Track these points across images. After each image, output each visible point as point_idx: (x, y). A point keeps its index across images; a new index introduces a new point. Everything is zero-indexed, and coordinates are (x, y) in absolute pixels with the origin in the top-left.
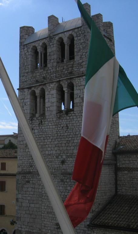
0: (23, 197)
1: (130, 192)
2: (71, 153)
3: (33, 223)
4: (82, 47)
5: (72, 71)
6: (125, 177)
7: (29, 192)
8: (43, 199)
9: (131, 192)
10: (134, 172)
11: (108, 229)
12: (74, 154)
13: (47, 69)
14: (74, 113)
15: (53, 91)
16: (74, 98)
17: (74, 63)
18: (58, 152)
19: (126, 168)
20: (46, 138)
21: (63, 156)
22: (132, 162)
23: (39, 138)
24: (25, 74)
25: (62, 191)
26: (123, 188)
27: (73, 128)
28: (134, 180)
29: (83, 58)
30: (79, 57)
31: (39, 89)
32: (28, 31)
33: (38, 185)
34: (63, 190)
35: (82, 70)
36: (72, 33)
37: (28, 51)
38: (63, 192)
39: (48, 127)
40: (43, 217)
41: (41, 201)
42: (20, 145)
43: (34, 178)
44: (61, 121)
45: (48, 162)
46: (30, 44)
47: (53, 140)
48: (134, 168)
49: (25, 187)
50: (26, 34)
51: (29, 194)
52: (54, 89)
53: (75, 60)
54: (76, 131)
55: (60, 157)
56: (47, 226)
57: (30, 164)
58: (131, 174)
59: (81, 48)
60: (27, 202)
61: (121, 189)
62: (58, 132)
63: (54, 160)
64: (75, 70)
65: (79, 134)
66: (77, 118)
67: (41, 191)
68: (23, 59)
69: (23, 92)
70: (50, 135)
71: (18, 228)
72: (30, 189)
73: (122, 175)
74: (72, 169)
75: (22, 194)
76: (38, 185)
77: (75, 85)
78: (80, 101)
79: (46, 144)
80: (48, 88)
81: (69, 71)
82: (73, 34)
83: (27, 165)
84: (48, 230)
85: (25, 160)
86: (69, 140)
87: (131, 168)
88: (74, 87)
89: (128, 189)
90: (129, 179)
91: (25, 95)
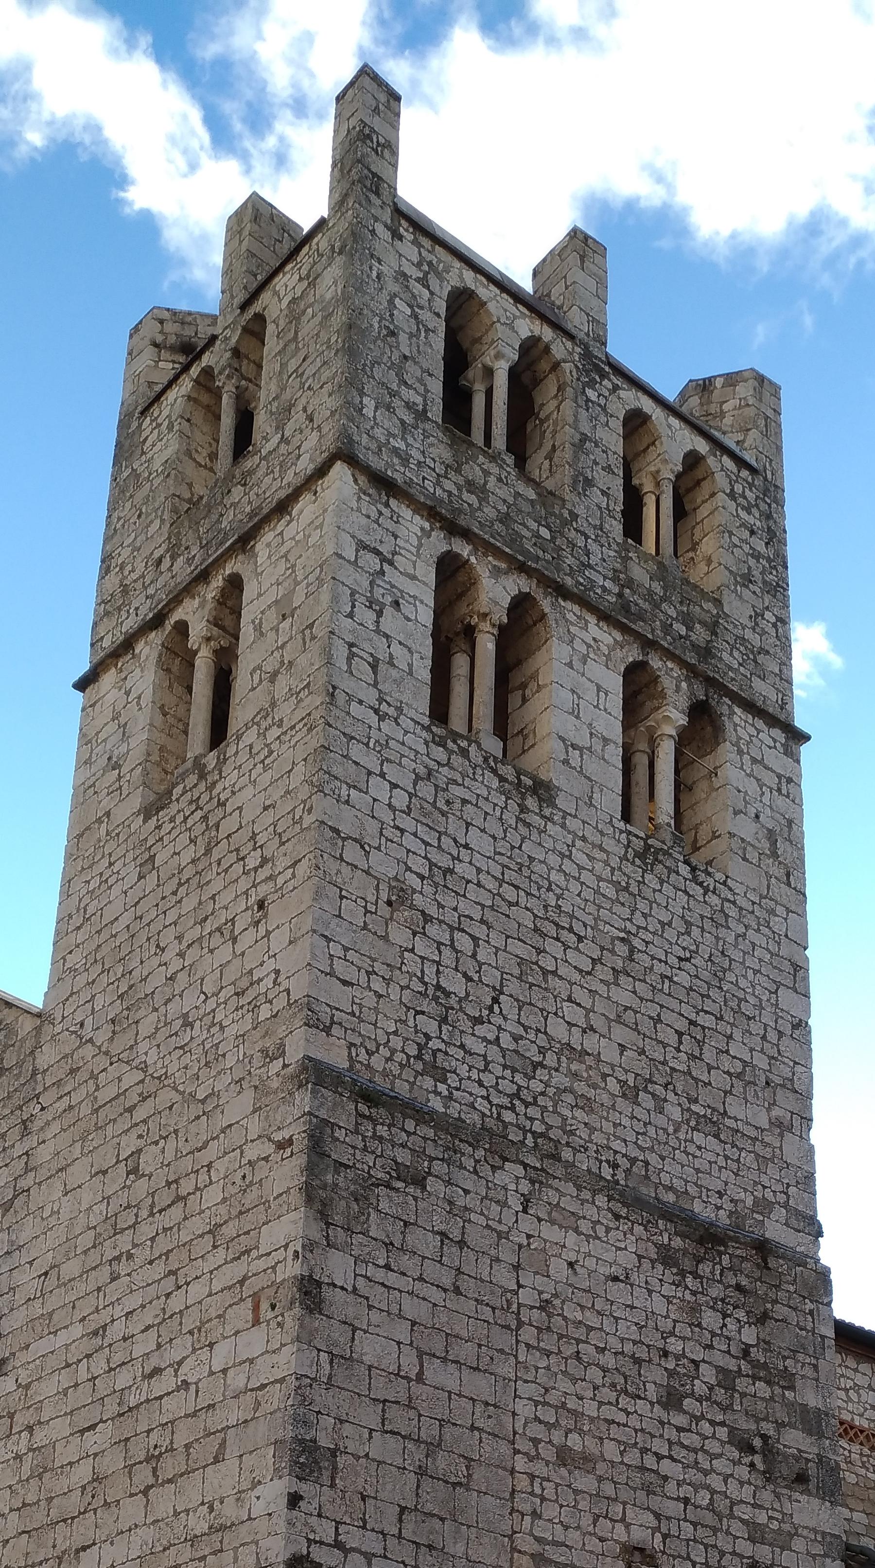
0: (361, 1282)
3: (442, 1520)
7: (417, 1260)
25: (670, 1324)
39: (568, 866)
43: (462, 1167)
45: (569, 1099)
57: (420, 1047)
63: (605, 1098)
76: (488, 1226)
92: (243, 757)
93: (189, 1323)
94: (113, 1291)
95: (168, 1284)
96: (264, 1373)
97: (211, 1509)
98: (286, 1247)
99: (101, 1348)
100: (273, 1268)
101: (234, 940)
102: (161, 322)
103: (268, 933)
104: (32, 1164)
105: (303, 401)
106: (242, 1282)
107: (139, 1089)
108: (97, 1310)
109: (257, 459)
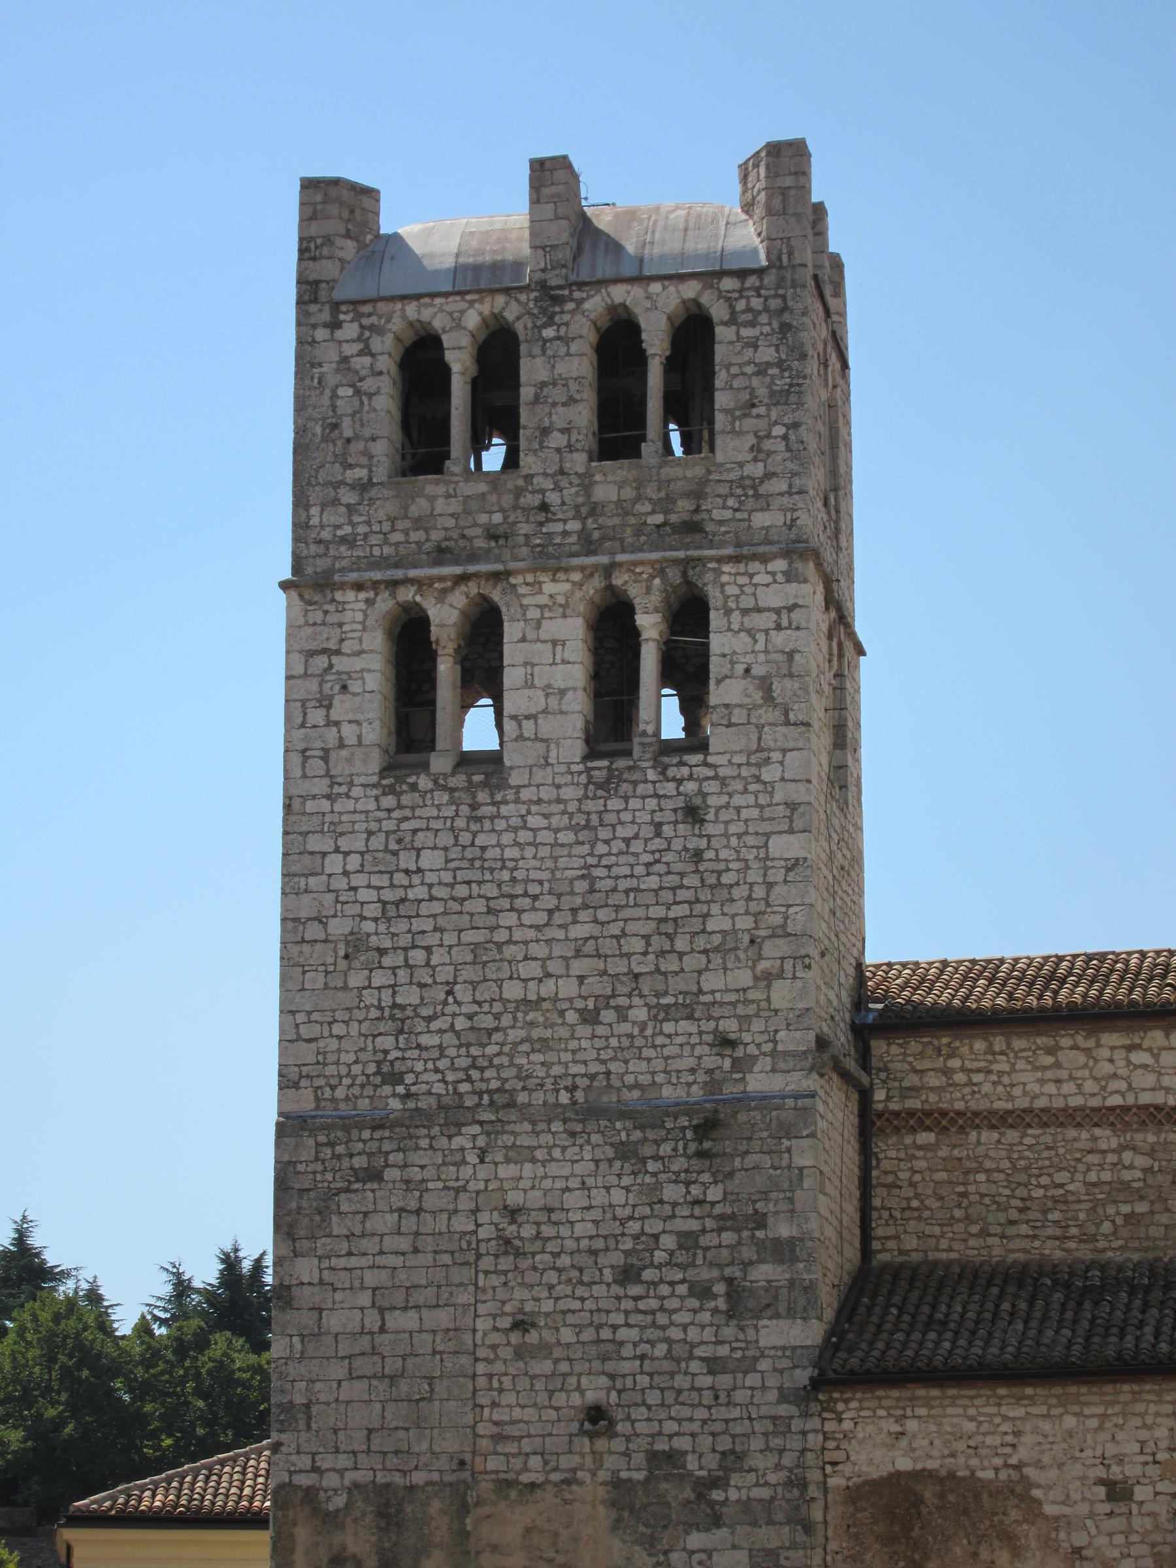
0: (326, 1273)
1: (950, 1250)
2: (686, 993)
3: (407, 1429)
4: (769, 387)
5: (696, 518)
6: (921, 1164)
7: (377, 1239)
8: (486, 1273)
9: (956, 1246)
10: (973, 1135)
11: (921, 1392)
12: (703, 999)
13: (521, 482)
14: (705, 764)
15: (560, 620)
16: (708, 678)
17: (709, 472)
18: (596, 985)
19: (928, 1114)
20: (505, 903)
21: (630, 1007)
22: (960, 1077)
23: (456, 907)
24: (343, 490)
26: (905, 1232)
27: (703, 851)
28: (971, 1178)
29: (769, 453)
30: (748, 445)
31: (459, 599)
32: (358, 215)
33: (446, 1188)
34: (634, 1206)
35: (761, 519)
36: (700, 293)
37: (367, 346)
38: (631, 1218)
39: (524, 836)
40: (482, 1382)
41: (471, 1288)
42: (306, 948)
43: (417, 1148)
44: (615, 804)
45: (525, 1047)
46: (382, 307)
47: (558, 918)
48: (976, 1114)
49: (344, 1207)
50: (348, 235)
51: (377, 1249)
52: (568, 612)
53: (720, 457)
54: (722, 866)
55: (608, 1016)
56: (508, 1430)
57: (379, 1063)
58: (955, 1146)
59: (762, 392)
60: (365, 1299)
61: (896, 1237)
62: (599, 872)
63: (564, 1032)
64: (717, 514)
65: (737, 884)
66: (730, 795)
67: (472, 1227)
68: (327, 392)
69: (331, 608)
70: (541, 882)
71: (291, 1473)
72: (382, 1222)
73: (902, 1154)
74: (689, 1085)
75: (320, 1258)
76: (446, 1188)
77: (719, 603)
78: (747, 696)
79: (510, 942)
80: (525, 601)
81: (673, 518)
82: (705, 300)
83: (357, 1069)
84: (527, 1455)
85: (340, 1038)
86: (675, 920)
87: (960, 1114)
88: (713, 615)
89: (937, 1230)
90: (943, 1175)
91: (340, 625)
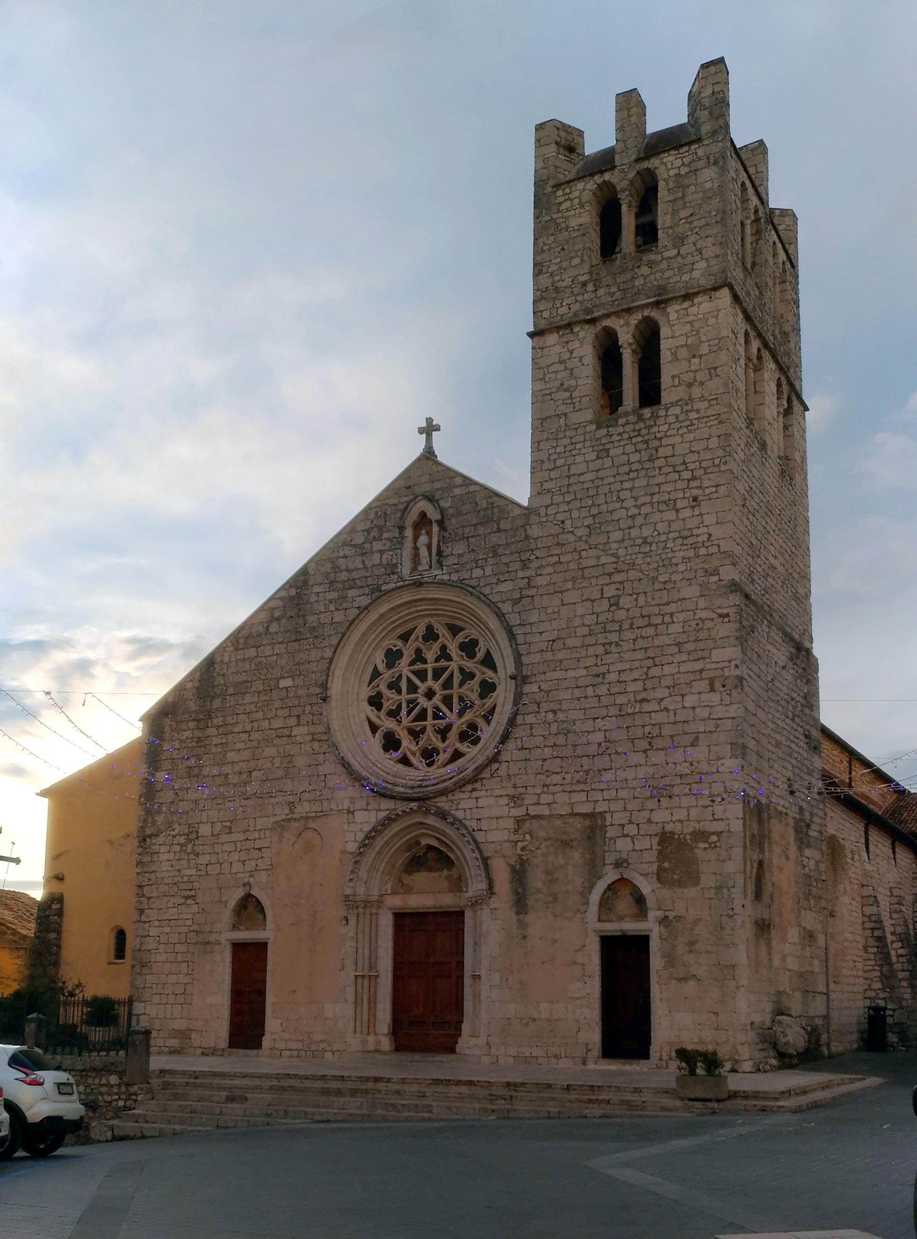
92: (672, 419)
93: (667, 681)
94: (607, 659)
95: (650, 663)
96: (720, 712)
97: (692, 764)
98: (730, 661)
99: (602, 683)
100: (722, 669)
101: (677, 511)
102: (558, 129)
103: (701, 515)
104: (532, 583)
105: (692, 239)
106: (701, 671)
107: (615, 566)
108: (596, 665)
109: (659, 257)
